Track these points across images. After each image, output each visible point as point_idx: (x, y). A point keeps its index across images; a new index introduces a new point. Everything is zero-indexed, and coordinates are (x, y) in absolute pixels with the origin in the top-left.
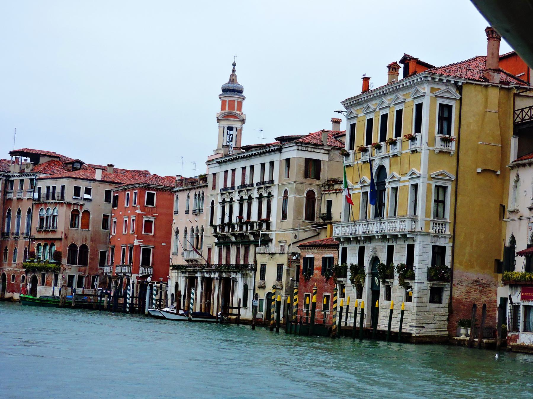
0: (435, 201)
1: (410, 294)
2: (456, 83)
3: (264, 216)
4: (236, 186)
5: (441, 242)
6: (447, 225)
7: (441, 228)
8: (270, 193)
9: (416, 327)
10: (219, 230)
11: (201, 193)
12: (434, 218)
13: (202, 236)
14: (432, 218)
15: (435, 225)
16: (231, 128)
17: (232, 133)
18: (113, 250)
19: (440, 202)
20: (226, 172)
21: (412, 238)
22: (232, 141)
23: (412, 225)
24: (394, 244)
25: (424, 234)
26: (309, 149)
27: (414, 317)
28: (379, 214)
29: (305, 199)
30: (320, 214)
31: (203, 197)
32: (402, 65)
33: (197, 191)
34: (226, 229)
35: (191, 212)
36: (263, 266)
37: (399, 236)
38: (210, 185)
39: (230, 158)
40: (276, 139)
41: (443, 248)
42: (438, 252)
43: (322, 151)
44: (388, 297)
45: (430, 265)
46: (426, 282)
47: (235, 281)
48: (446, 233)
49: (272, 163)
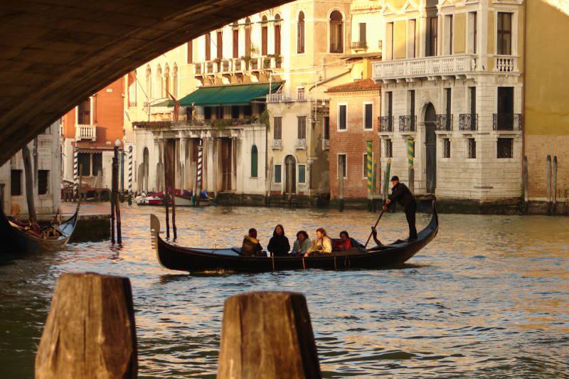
0: (499, 32)
6: (515, 62)
8: (278, 16)
9: (482, 188)
12: (498, 54)
13: (175, 77)
14: (496, 54)
15: (499, 62)
21: (473, 79)
23: (471, 63)
24: (452, 86)
27: (479, 176)
28: (430, 51)
29: (328, 24)
30: (349, 43)
36: (278, 121)
41: (511, 89)
42: (505, 95)
45: (496, 112)
47: (237, 141)
48: (514, 71)
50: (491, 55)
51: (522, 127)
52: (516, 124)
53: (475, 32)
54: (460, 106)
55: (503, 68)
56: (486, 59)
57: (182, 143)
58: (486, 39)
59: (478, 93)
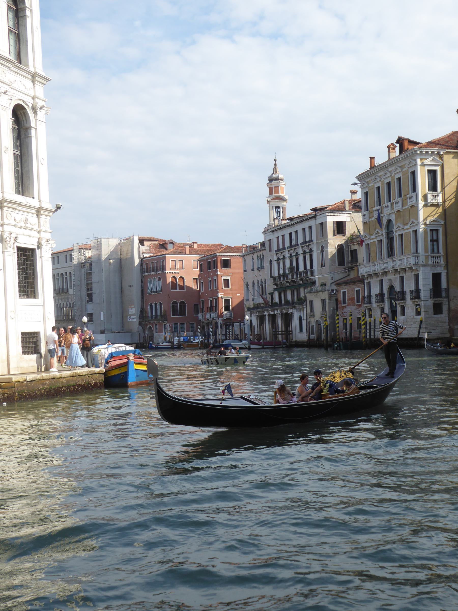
0: (431, 241)
1: (419, 310)
2: (438, 153)
3: (308, 267)
4: (286, 246)
5: (438, 270)
7: (437, 260)
8: (311, 249)
10: (277, 280)
11: (261, 255)
13: (265, 286)
14: (430, 253)
16: (278, 207)
17: (279, 210)
18: (203, 302)
19: (434, 241)
20: (278, 238)
22: (279, 216)
23: (415, 260)
24: (404, 275)
25: (425, 265)
26: (336, 214)
31: (263, 258)
32: (398, 145)
33: (259, 254)
34: (282, 279)
35: (255, 269)
36: (311, 302)
37: (407, 269)
38: (268, 248)
39: (279, 227)
40: (311, 210)
42: (436, 277)
43: (346, 215)
44: (403, 314)
45: (432, 287)
46: (430, 300)
47: (292, 314)
49: (310, 228)
50: (427, 254)
51: (448, 296)
52: (444, 294)
53: (416, 242)
54: (409, 286)
55: (434, 262)
56: (424, 257)
57: (267, 317)
58: (424, 246)
59: (421, 277)
